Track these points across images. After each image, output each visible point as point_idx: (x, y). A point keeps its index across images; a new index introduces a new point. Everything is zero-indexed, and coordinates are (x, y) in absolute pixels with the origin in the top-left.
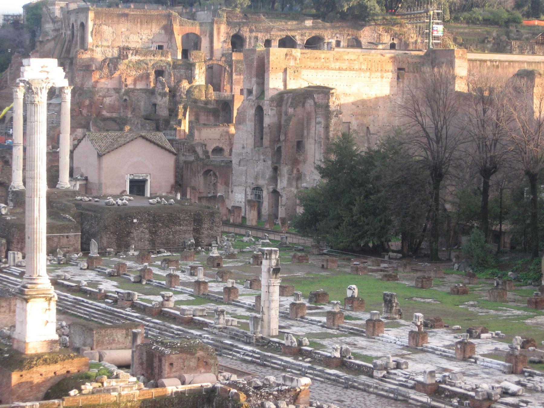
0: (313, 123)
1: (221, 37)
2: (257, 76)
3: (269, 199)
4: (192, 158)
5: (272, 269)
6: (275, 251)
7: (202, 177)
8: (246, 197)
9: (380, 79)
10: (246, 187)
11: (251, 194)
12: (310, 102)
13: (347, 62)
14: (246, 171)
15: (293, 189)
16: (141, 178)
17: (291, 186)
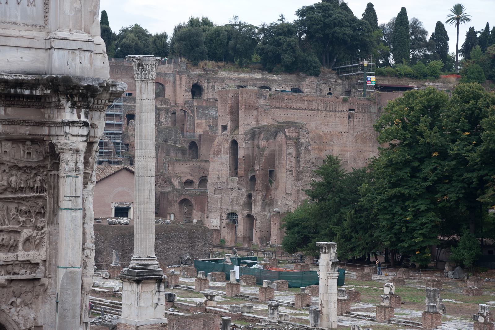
0: (284, 154)
1: (182, 86)
2: (232, 113)
3: (244, 223)
4: (169, 189)
5: (331, 263)
6: (334, 245)
7: (178, 205)
8: (221, 222)
9: (334, 118)
10: (221, 213)
11: (226, 219)
12: (281, 135)
13: (306, 102)
14: (221, 198)
15: (266, 213)
16: (125, 206)
17: (265, 211)
